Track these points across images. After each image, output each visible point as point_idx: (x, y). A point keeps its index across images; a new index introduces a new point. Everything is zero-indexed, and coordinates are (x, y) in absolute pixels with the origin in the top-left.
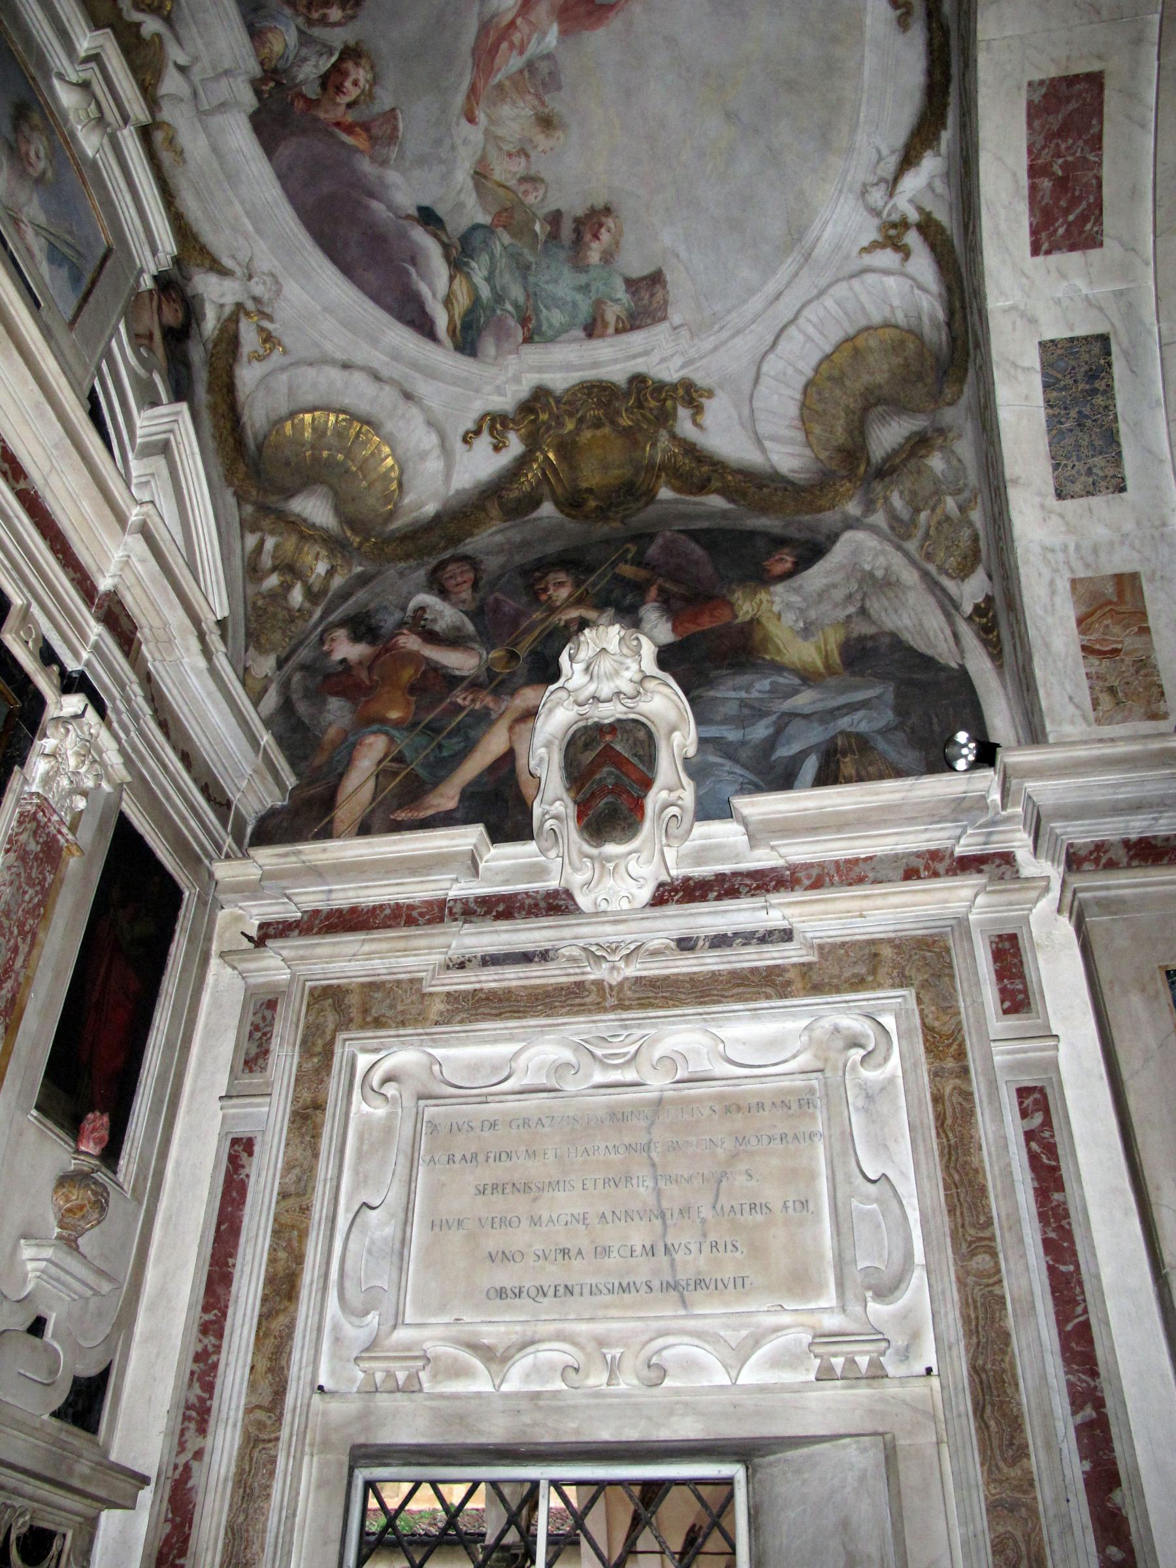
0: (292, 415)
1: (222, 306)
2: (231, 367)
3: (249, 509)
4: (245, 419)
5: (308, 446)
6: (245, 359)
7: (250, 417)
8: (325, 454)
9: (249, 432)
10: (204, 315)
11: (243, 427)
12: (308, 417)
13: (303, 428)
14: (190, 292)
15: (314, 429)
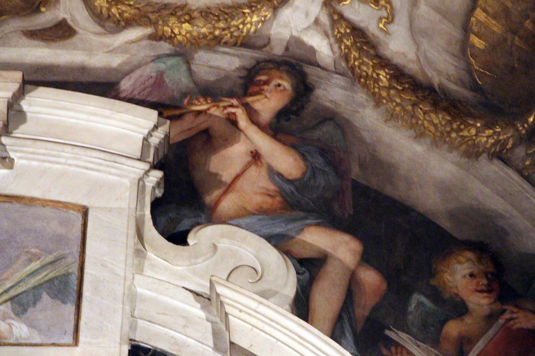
0: (466, 29)
1: (317, 22)
2: (378, 56)
3: (520, 151)
4: (436, 80)
5: (509, 36)
6: (381, 35)
7: (439, 73)
8: (528, 24)
9: (453, 87)
10: (312, 50)
11: (445, 91)
12: (479, 14)
13: (487, 27)
14: (278, 50)
15: (495, 17)
